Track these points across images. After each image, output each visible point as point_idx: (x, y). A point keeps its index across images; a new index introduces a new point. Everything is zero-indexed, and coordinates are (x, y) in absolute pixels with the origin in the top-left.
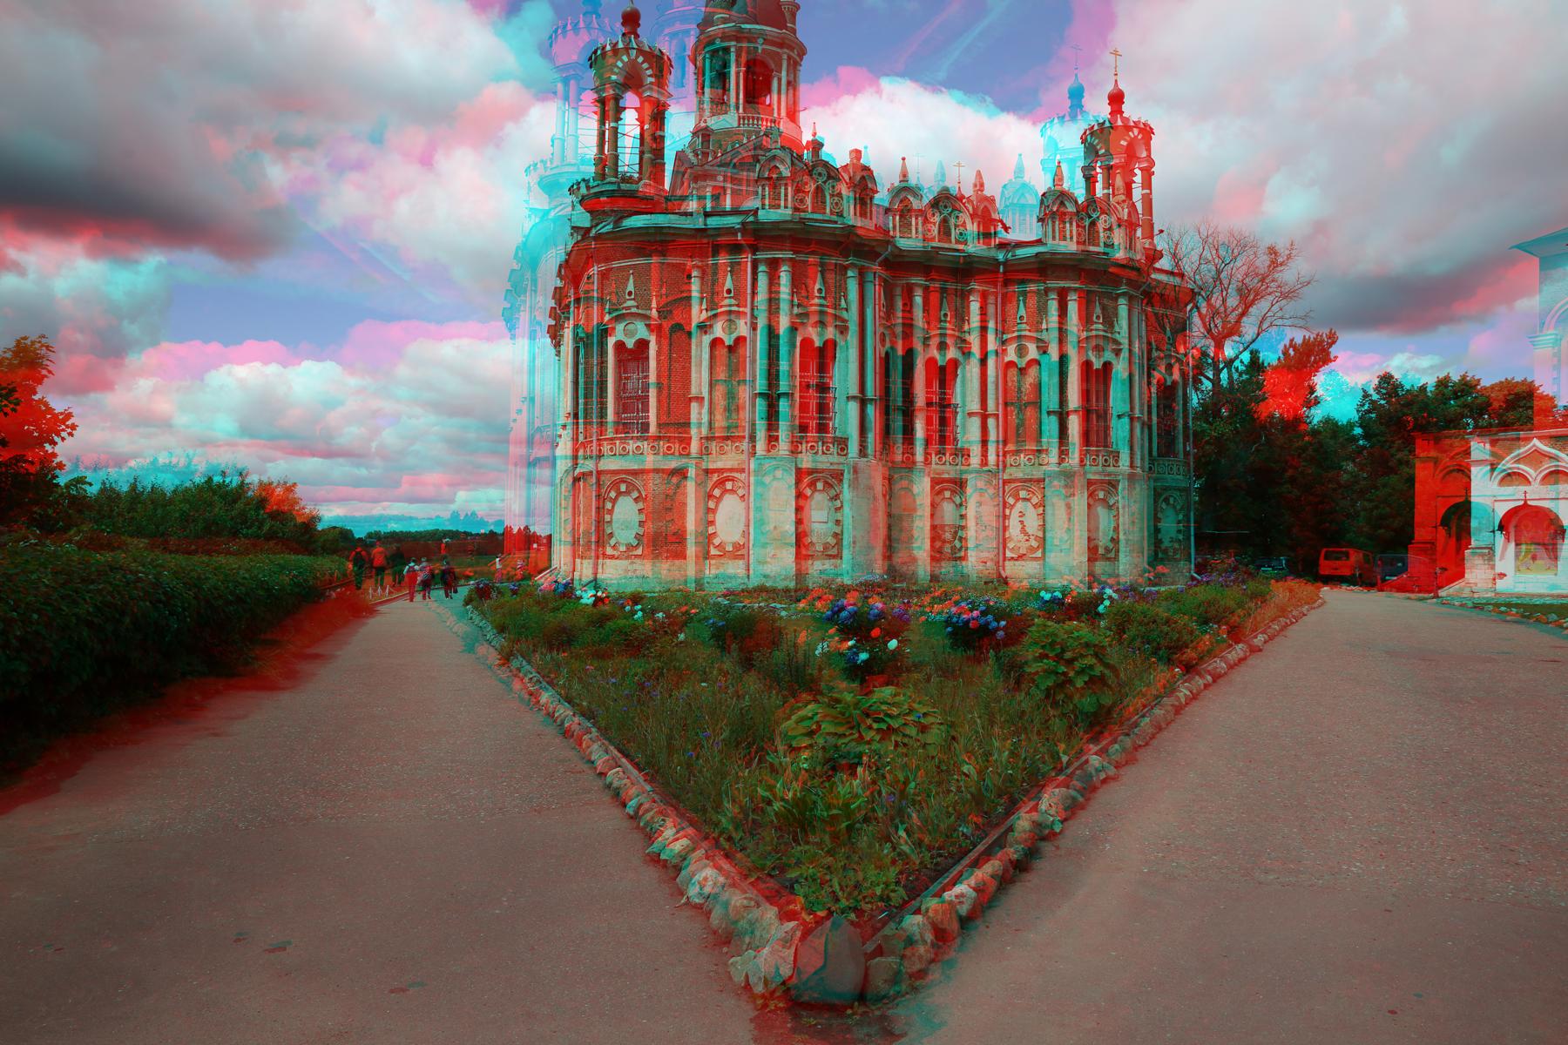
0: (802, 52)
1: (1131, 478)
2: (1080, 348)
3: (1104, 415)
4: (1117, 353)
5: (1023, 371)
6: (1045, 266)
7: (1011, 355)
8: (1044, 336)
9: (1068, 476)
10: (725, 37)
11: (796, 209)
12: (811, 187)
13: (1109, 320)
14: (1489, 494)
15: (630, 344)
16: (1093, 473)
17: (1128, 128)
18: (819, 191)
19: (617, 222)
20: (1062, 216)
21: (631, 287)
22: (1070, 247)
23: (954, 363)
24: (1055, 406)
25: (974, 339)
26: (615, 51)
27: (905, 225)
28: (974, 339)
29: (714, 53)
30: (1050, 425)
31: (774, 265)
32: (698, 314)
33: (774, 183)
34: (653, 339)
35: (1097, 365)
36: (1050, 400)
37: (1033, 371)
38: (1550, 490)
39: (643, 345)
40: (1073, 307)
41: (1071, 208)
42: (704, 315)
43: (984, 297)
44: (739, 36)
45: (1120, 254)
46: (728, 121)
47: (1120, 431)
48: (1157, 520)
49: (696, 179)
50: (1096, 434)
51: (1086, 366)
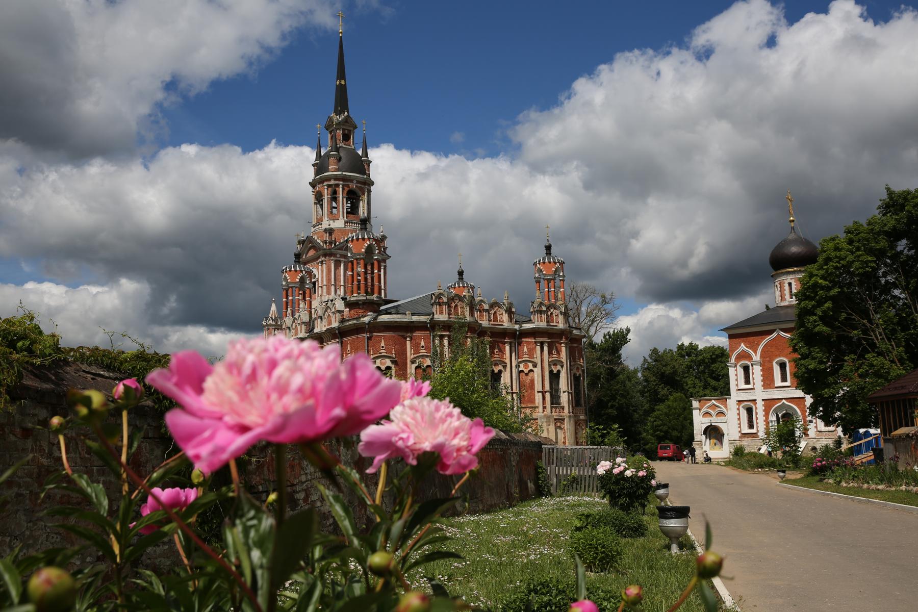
0: (373, 183)
1: (570, 416)
2: (550, 366)
3: (558, 390)
4: (562, 366)
5: (527, 374)
6: (534, 333)
7: (522, 368)
8: (535, 360)
9: (548, 417)
10: (336, 178)
11: (449, 314)
12: (453, 305)
13: (558, 353)
14: (700, 422)
15: (383, 368)
16: (555, 415)
17: (555, 263)
18: (456, 306)
19: (375, 318)
20: (541, 312)
21: (383, 344)
22: (543, 325)
23: (500, 372)
24: (540, 389)
25: (508, 361)
26: (363, 239)
27: (482, 315)
28: (508, 361)
29: (329, 186)
30: (538, 398)
31: (442, 337)
32: (410, 355)
33: (440, 304)
34: (393, 366)
35: (555, 372)
36: (538, 386)
37: (531, 374)
38: (720, 419)
39: (388, 368)
40: (546, 349)
41: (544, 308)
42: (413, 356)
43: (510, 344)
44: (344, 179)
45: (561, 326)
46: (339, 224)
47: (564, 398)
48: (576, 433)
49: (325, 255)
50: (555, 400)
51: (551, 372)
